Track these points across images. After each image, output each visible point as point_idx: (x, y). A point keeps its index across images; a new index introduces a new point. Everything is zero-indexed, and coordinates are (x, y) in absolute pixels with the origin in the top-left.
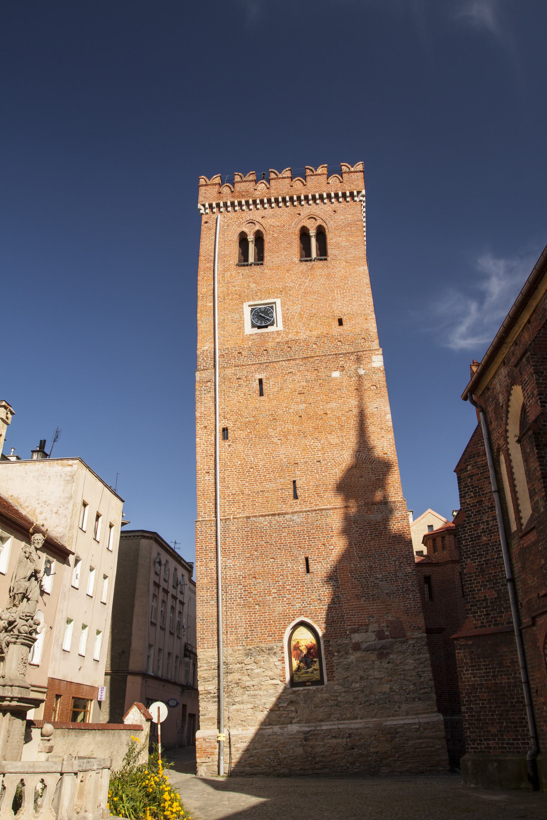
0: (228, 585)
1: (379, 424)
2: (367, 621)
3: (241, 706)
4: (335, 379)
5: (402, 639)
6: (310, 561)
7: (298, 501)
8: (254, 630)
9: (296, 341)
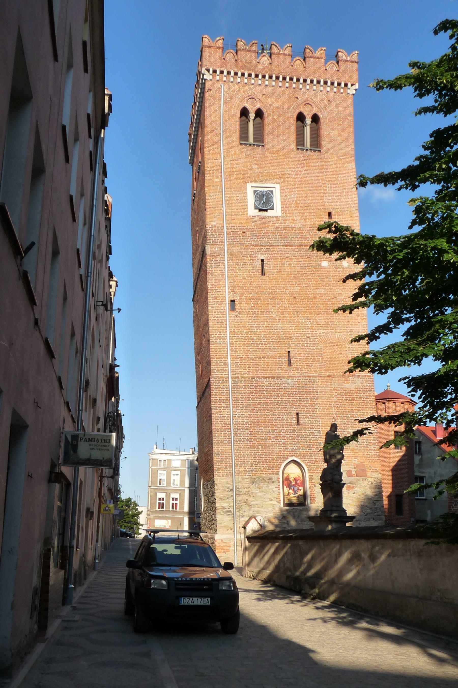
4: (324, 268)
5: (365, 478)
6: (300, 416)
7: (292, 368)
9: (293, 228)
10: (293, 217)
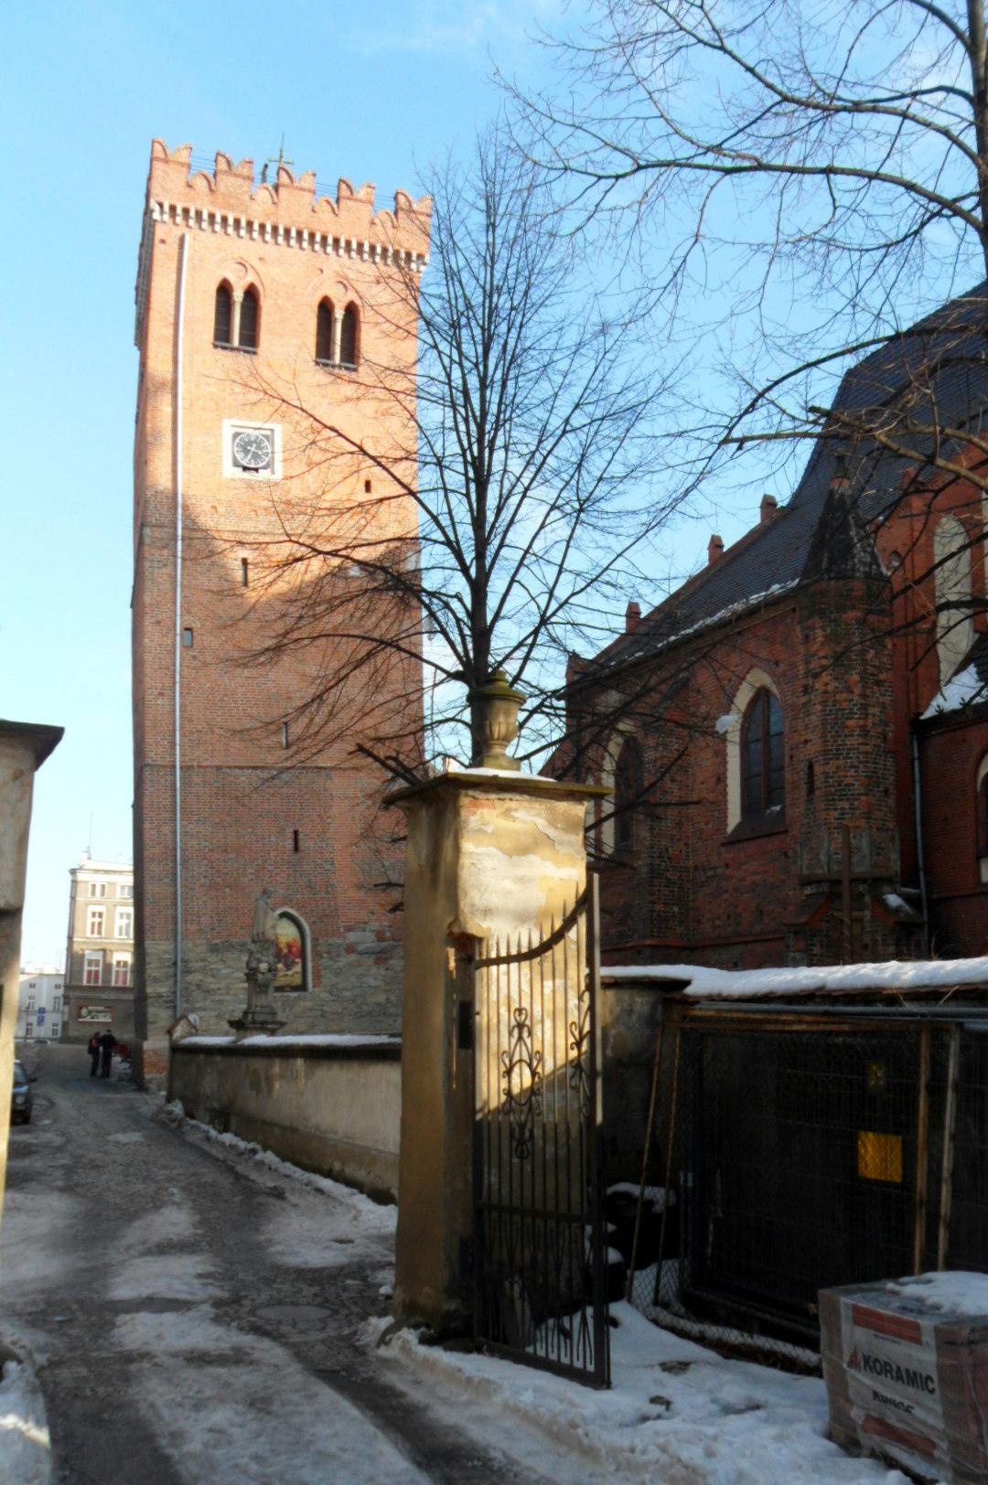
6: (301, 836)
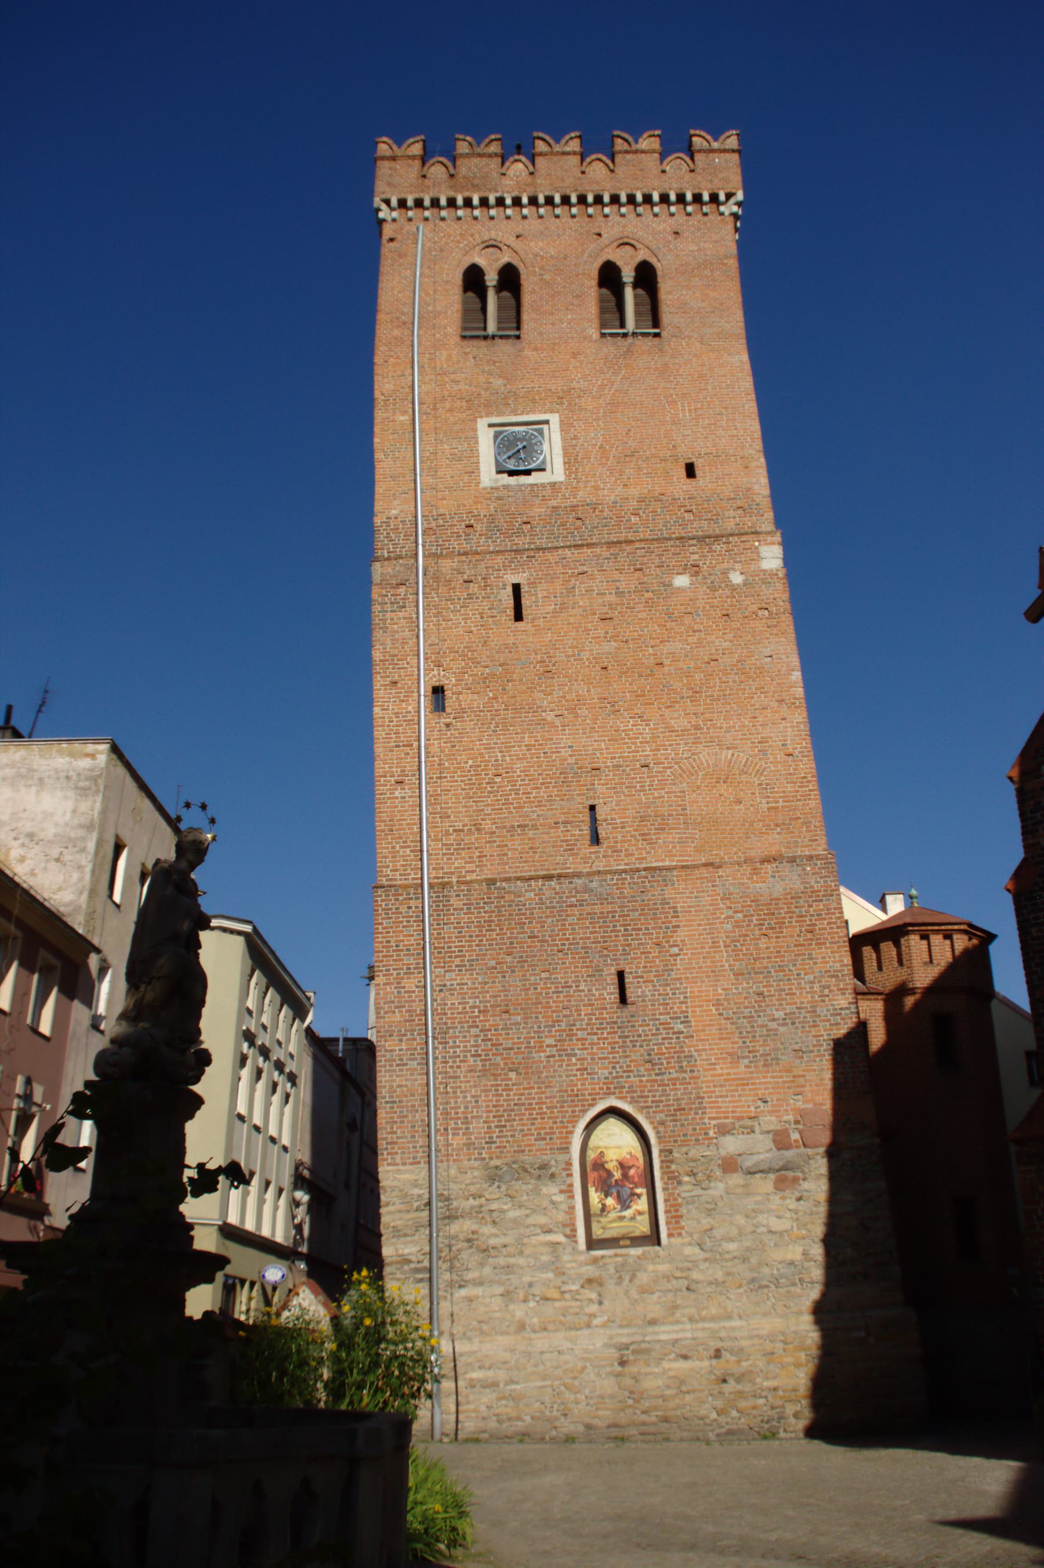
0: (448, 1028)
1: (775, 692)
2: (752, 1109)
3: (479, 1291)
7: (601, 849)
8: (505, 1126)
10: (596, 481)
